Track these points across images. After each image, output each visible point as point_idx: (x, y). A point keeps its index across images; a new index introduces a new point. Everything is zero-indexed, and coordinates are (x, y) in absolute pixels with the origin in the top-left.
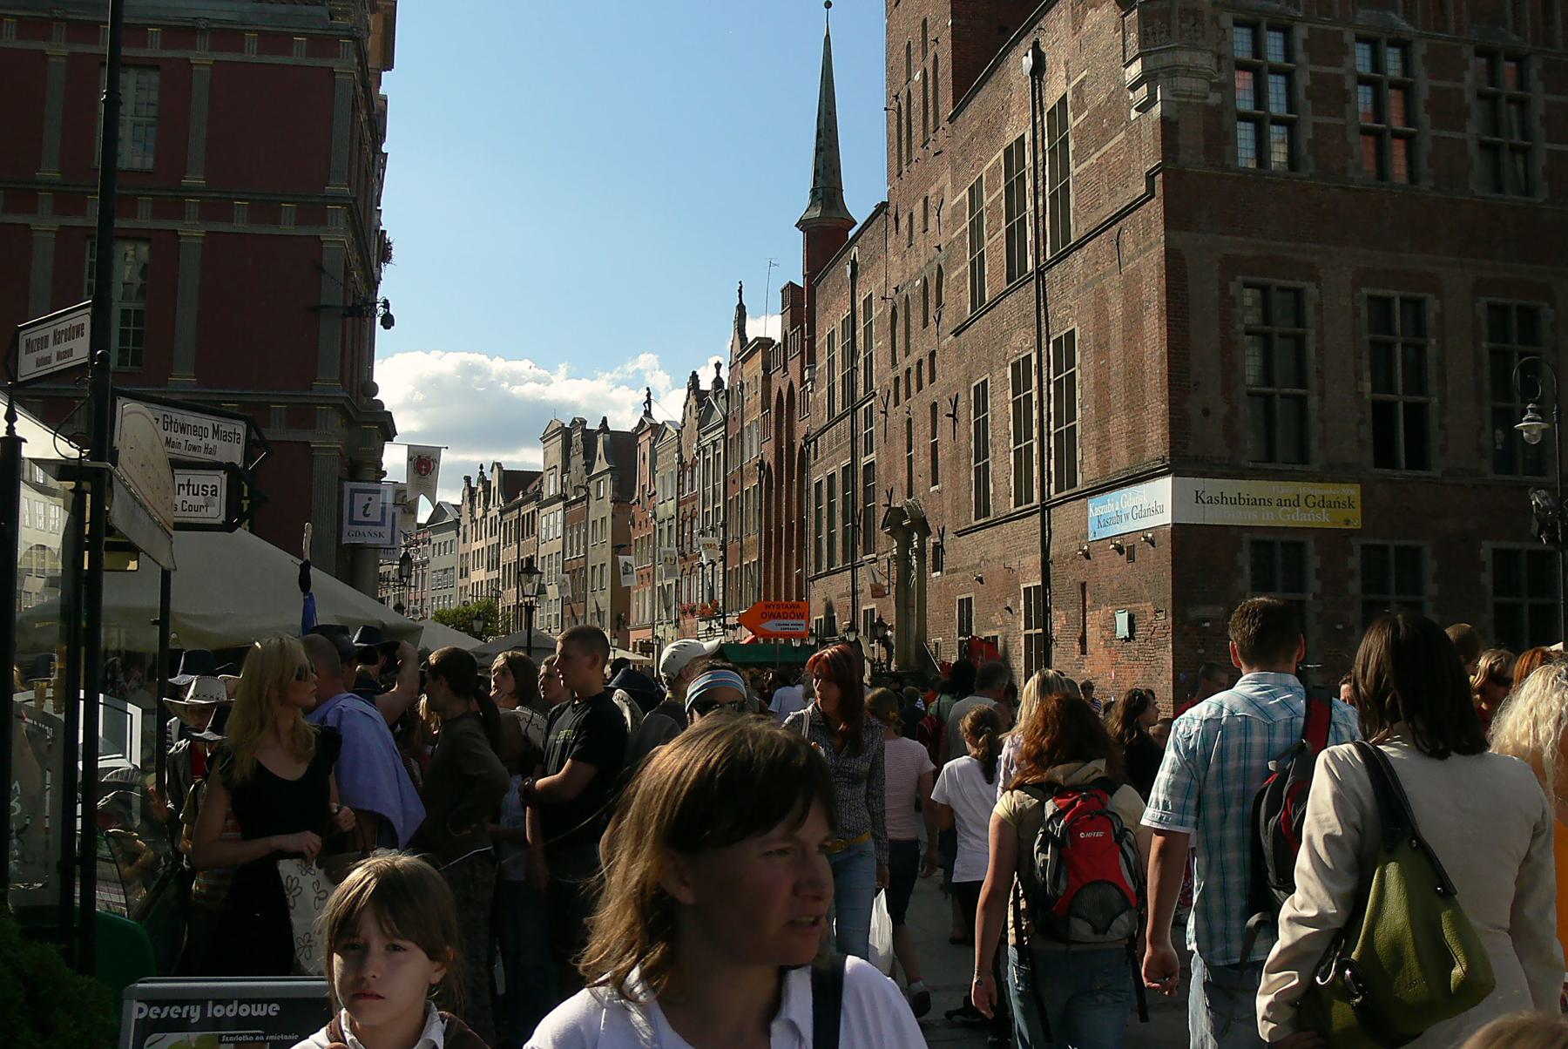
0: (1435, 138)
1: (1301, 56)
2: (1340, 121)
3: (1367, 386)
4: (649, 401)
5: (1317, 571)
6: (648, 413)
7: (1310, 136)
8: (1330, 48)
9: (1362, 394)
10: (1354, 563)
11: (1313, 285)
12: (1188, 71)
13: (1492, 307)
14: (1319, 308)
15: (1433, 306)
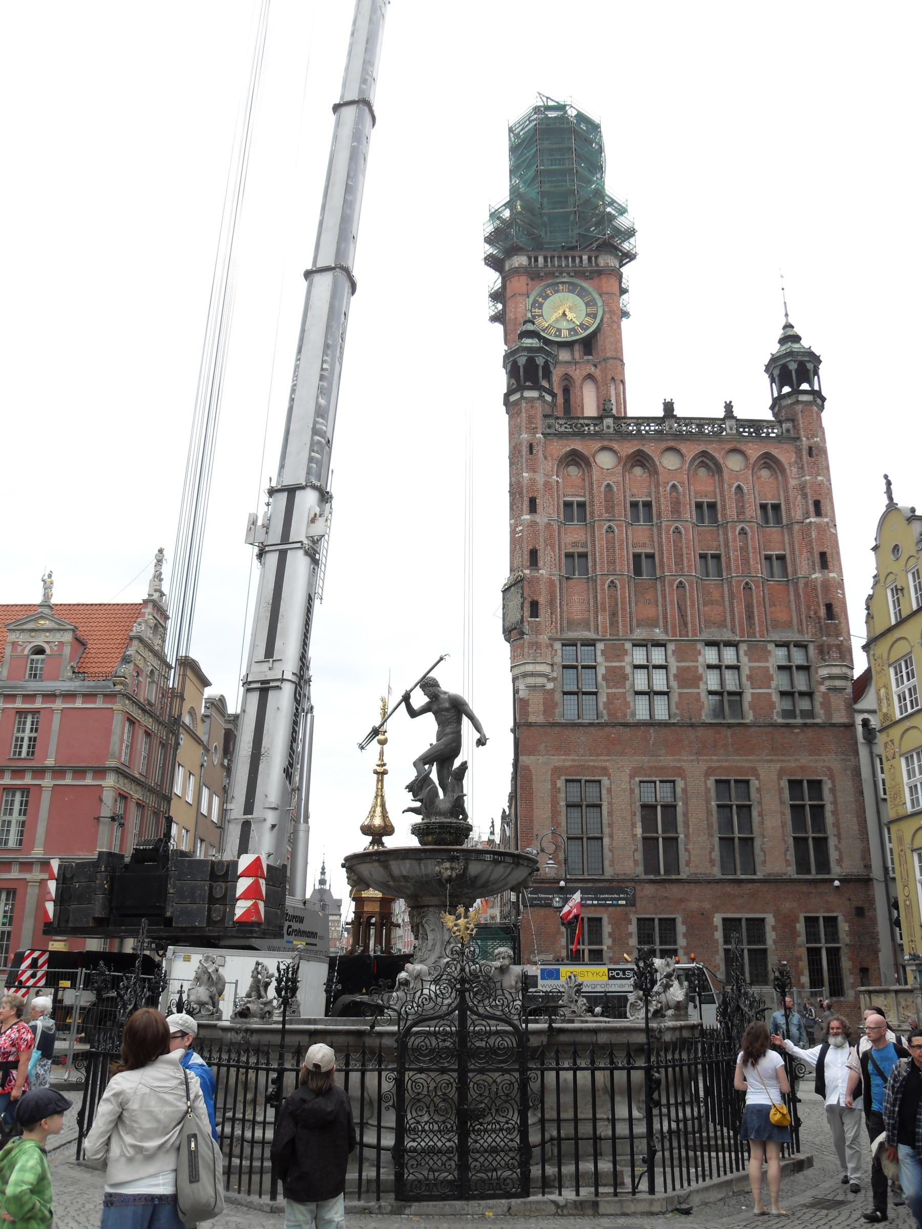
0: (680, 694)
1: (600, 659)
2: (623, 690)
3: (639, 831)
4: (493, 826)
5: (609, 933)
6: (492, 833)
7: (605, 700)
8: (616, 652)
9: (636, 835)
10: (633, 928)
11: (606, 778)
12: (532, 675)
13: (717, 781)
14: (609, 791)
15: (680, 784)
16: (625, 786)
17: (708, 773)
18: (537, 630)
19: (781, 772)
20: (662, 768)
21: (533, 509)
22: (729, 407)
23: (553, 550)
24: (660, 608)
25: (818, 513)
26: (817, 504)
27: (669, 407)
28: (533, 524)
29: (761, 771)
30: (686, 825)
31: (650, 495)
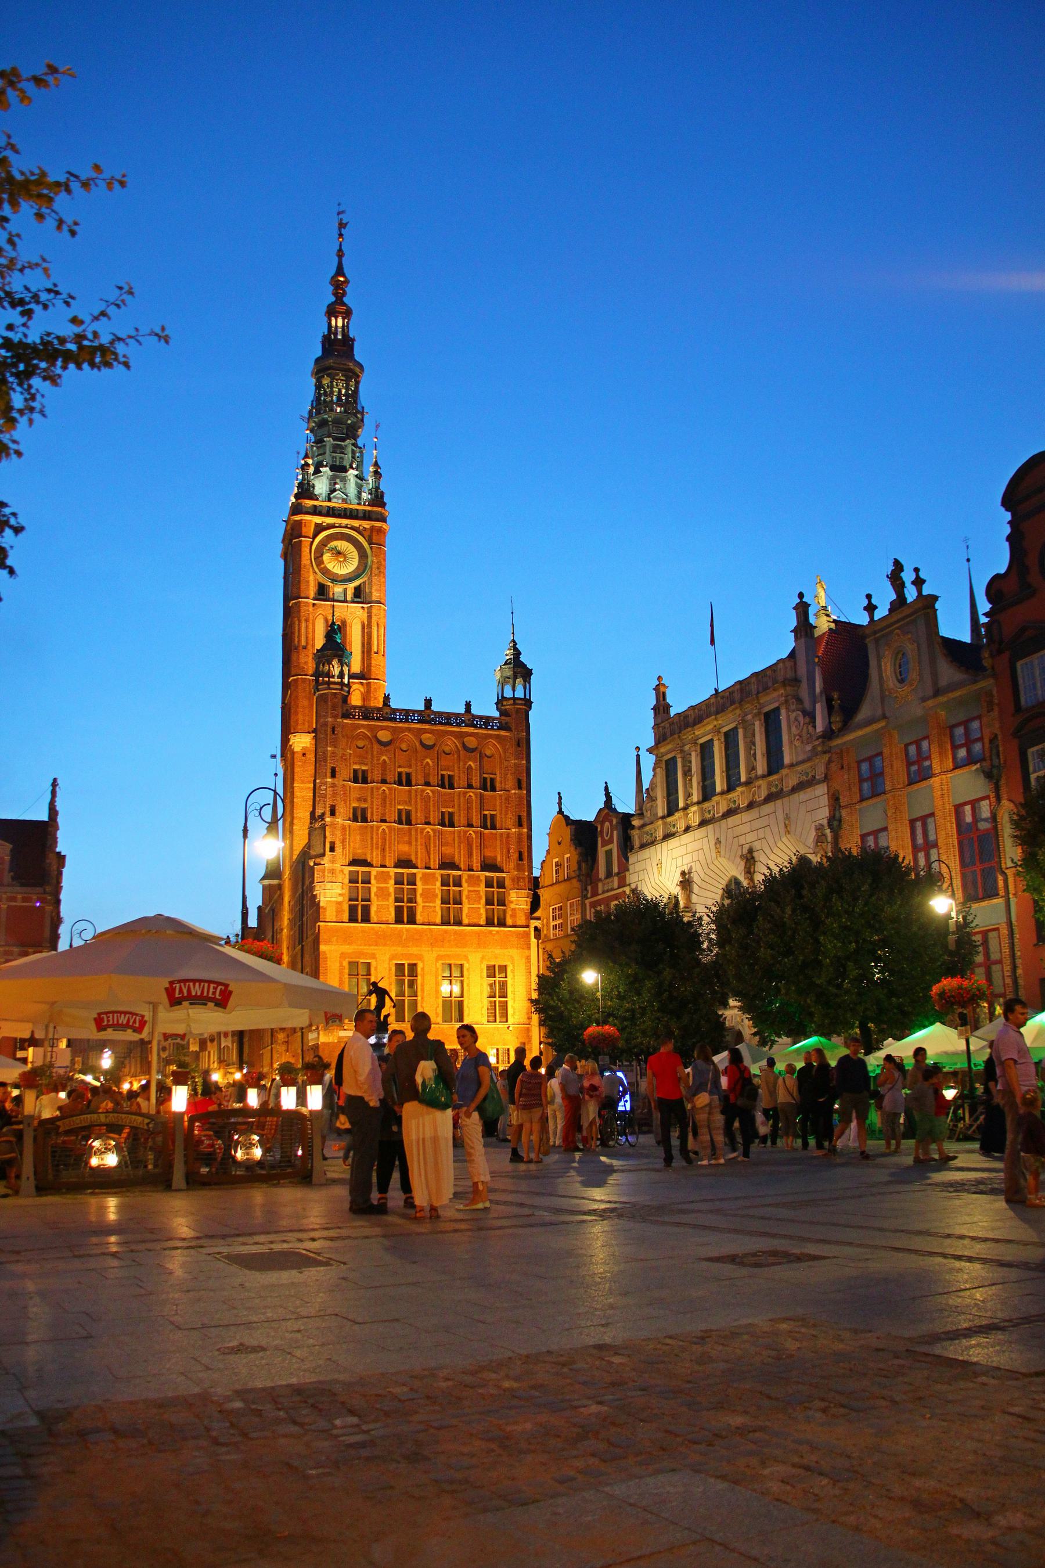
14: (376, 968)
16: (386, 965)
17: (439, 958)
18: (333, 862)
19: (483, 958)
20: (411, 954)
21: (333, 775)
22: (468, 705)
23: (345, 802)
24: (413, 848)
25: (520, 788)
26: (519, 781)
27: (428, 703)
28: (333, 785)
29: (470, 957)
30: (423, 990)
31: (410, 767)
